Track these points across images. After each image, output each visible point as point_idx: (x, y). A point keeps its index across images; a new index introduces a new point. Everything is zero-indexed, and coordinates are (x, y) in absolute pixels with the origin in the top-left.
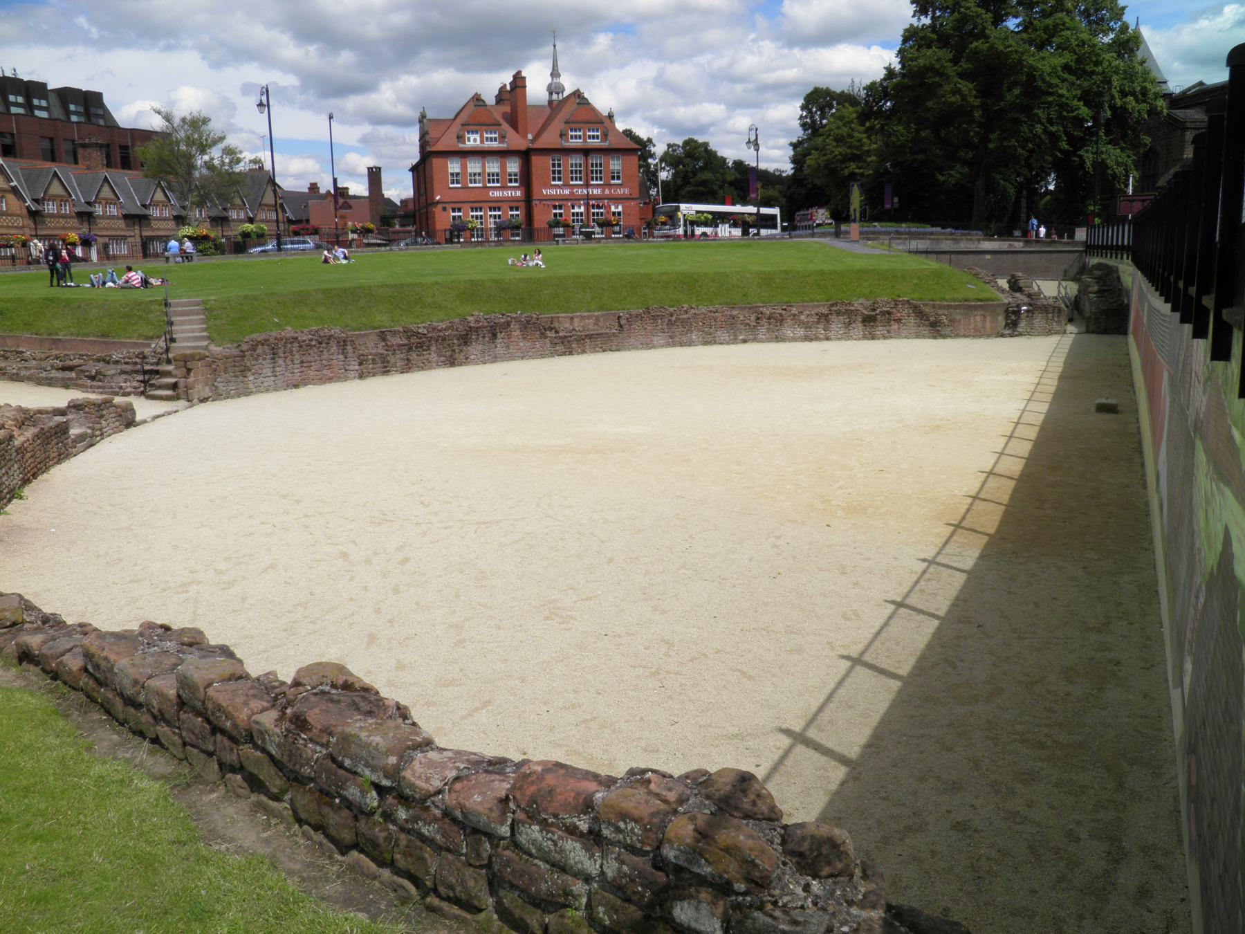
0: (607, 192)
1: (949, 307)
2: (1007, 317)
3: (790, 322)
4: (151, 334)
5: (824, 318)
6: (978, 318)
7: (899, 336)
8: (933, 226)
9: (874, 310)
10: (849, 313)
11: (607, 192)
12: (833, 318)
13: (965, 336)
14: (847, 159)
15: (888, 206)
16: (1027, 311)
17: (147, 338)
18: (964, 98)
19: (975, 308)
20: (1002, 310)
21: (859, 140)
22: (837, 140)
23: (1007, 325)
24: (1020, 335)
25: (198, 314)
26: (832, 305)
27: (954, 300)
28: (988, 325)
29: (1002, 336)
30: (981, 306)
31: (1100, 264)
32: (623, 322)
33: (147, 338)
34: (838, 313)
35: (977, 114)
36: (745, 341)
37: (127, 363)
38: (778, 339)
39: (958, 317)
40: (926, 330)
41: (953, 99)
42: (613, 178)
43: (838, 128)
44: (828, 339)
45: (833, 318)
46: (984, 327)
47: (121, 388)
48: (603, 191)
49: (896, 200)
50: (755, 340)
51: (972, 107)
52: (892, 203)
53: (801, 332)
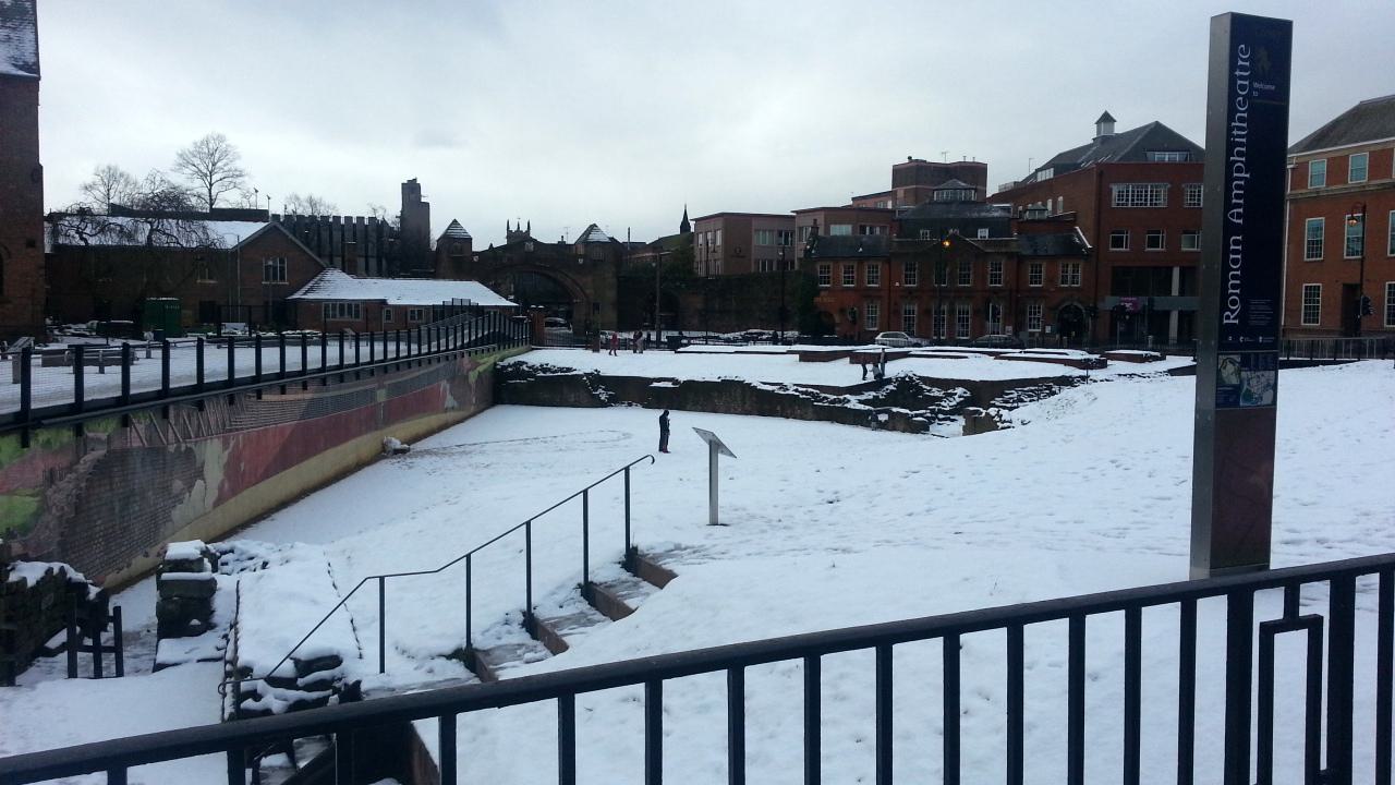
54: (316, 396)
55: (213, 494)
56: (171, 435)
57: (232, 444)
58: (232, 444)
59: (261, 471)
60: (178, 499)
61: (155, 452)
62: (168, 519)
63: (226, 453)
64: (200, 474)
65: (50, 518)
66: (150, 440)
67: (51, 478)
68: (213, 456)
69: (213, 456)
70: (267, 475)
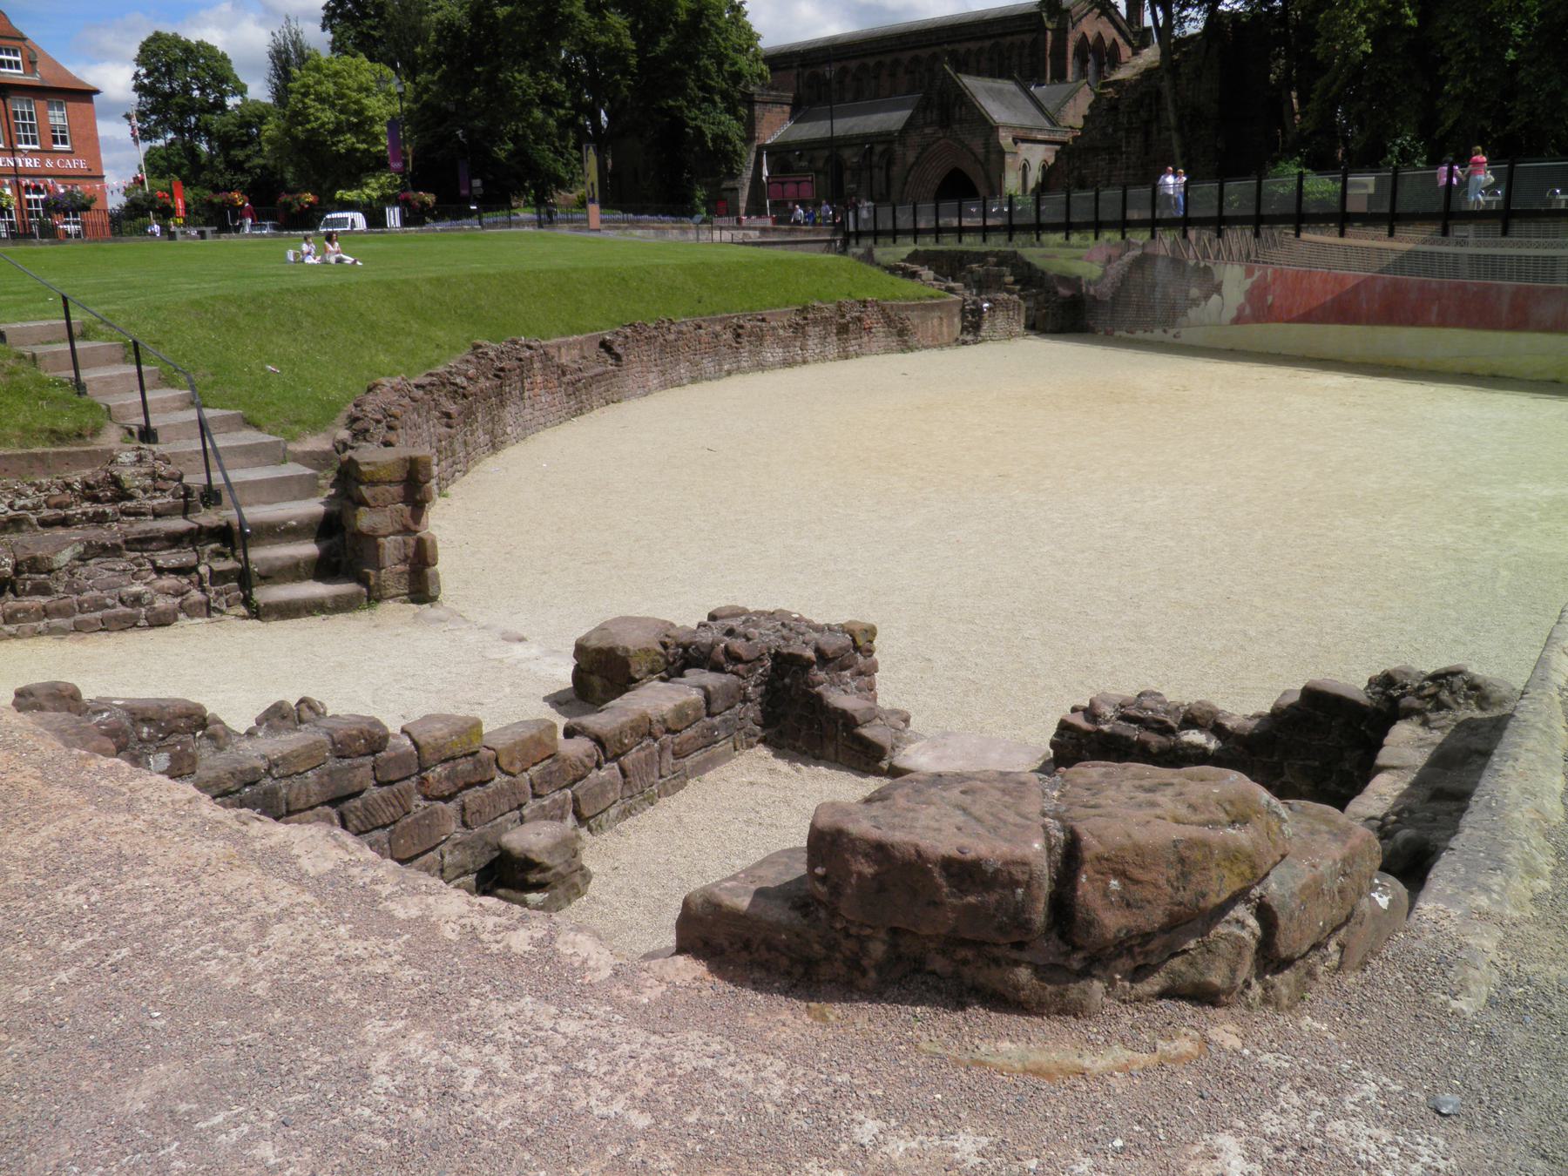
0: (49, 164)
1: (907, 308)
2: (963, 318)
3: (769, 339)
4: (65, 424)
5: (799, 330)
6: (936, 322)
7: (871, 353)
8: (624, 211)
9: (843, 316)
10: (826, 321)
11: (49, 164)
12: (811, 330)
13: (926, 347)
14: (338, 130)
15: (464, 192)
16: (989, 309)
17: (56, 436)
18: (617, 35)
19: (932, 307)
20: (956, 310)
21: (357, 102)
22: (320, 99)
23: (964, 329)
24: (984, 340)
25: (111, 362)
26: (802, 311)
27: (906, 298)
28: (945, 329)
29: (965, 343)
30: (938, 305)
31: (916, 252)
32: (619, 350)
33: (56, 436)
34: (815, 322)
35: (633, 61)
36: (729, 373)
37: (45, 523)
38: (761, 367)
39: (916, 321)
40: (893, 341)
41: (603, 39)
42: (55, 141)
43: (319, 82)
44: (805, 362)
45: (811, 330)
46: (941, 333)
47: (137, 600)
48: (42, 163)
49: (477, 183)
50: (739, 370)
51: (627, 50)
52: (471, 188)
53: (779, 353)
54: (1426, 248)
55: (1231, 313)
56: (1191, 252)
57: (1257, 274)
58: (1257, 274)
59: (1295, 314)
60: (1195, 303)
61: (1177, 262)
62: (1185, 314)
63: (1249, 281)
64: (1218, 289)
65: (1108, 281)
66: (1173, 252)
67: (1109, 260)
68: (1235, 281)
69: (1235, 281)
70: (1307, 317)
